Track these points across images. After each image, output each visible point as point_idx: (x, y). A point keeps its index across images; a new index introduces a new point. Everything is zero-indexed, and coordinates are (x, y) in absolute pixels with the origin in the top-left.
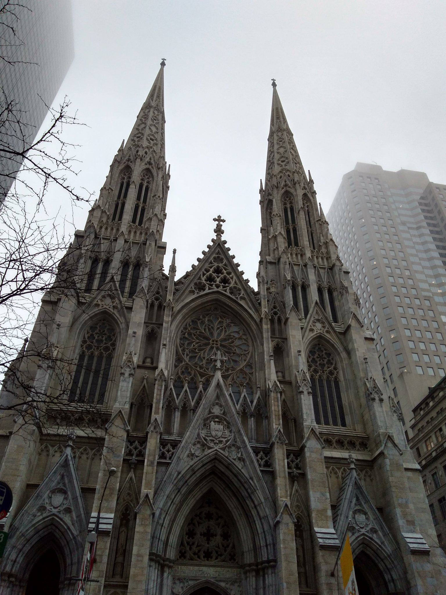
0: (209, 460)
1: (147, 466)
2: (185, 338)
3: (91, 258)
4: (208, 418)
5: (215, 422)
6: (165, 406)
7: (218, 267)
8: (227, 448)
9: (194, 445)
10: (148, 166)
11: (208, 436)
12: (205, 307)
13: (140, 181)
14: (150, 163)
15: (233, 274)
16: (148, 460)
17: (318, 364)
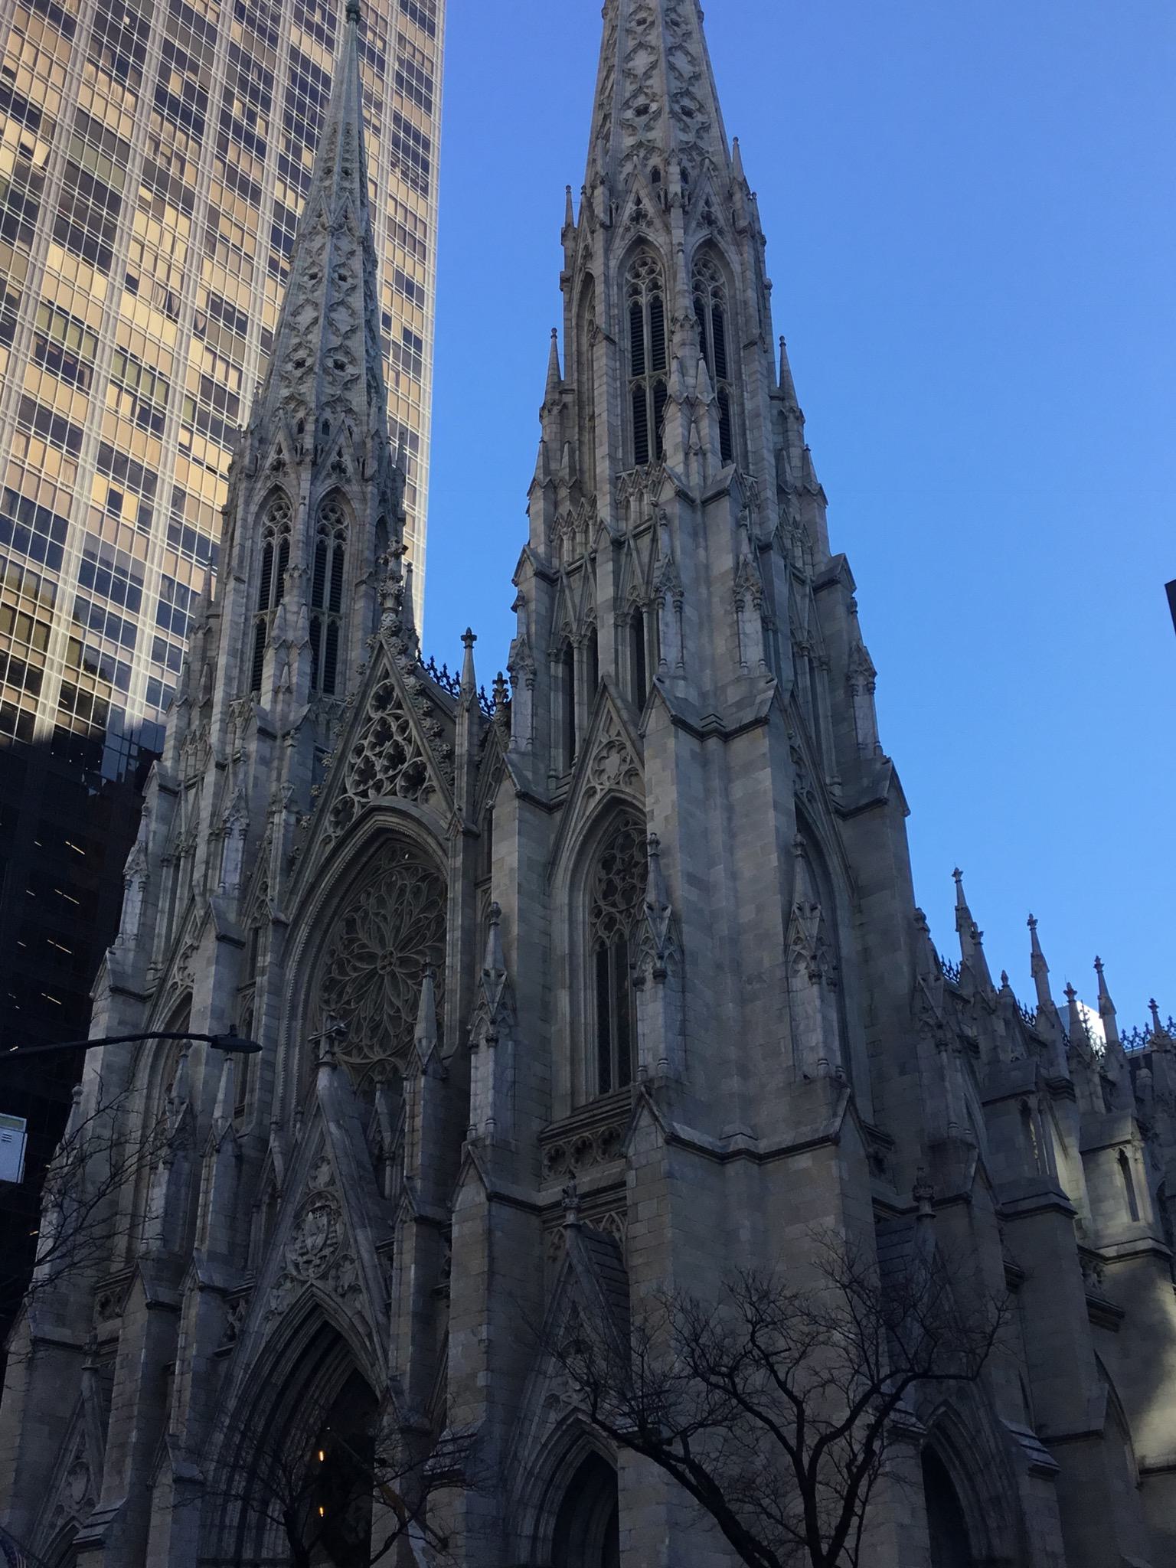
0: (303, 1313)
1: (182, 1374)
2: (332, 980)
3: (168, 861)
4: (303, 1208)
5: (313, 1212)
6: (266, 1199)
7: (383, 722)
8: (333, 1272)
9: (279, 1286)
10: (269, 484)
11: (302, 1255)
12: (367, 862)
13: (261, 544)
14: (278, 466)
15: (411, 724)
16: (183, 1361)
17: (617, 898)
